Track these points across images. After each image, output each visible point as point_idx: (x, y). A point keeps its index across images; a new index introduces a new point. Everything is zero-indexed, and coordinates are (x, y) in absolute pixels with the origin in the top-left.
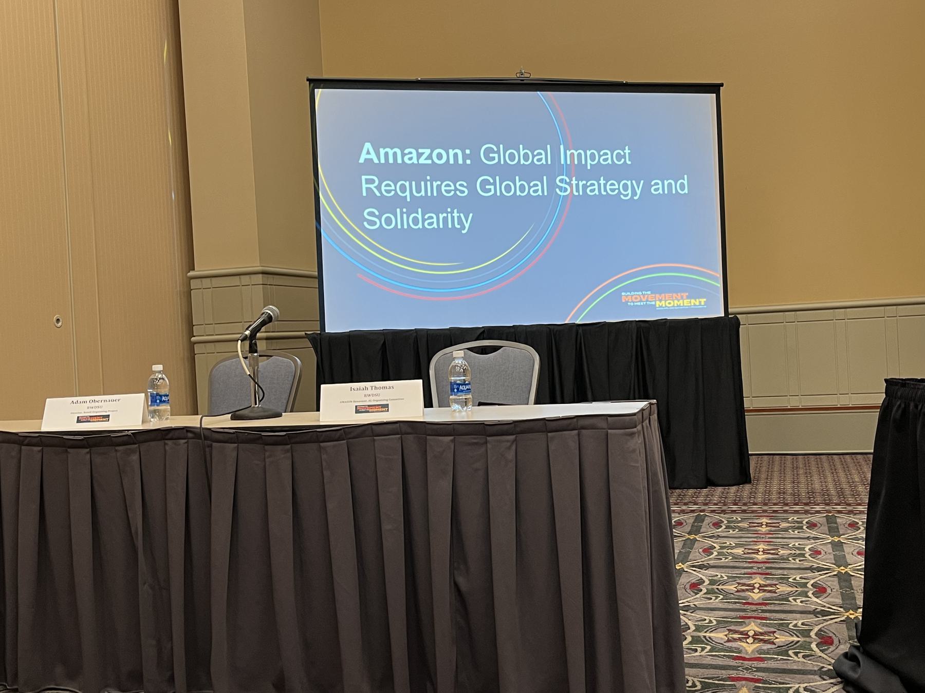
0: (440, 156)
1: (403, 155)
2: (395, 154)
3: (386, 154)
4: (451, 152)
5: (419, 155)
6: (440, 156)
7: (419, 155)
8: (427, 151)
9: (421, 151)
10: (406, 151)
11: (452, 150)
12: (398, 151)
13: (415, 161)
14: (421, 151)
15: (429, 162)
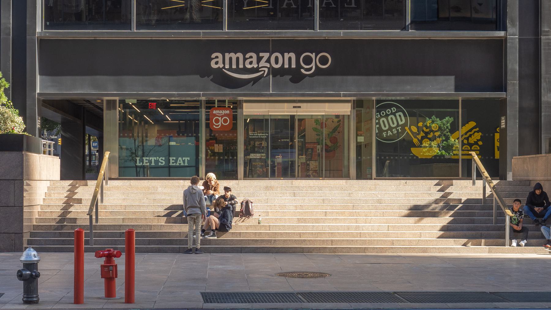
1: (245, 59)
2: (238, 59)
3: (231, 59)
8: (266, 55)
9: (261, 54)
10: (248, 56)
11: (287, 53)
12: (240, 55)
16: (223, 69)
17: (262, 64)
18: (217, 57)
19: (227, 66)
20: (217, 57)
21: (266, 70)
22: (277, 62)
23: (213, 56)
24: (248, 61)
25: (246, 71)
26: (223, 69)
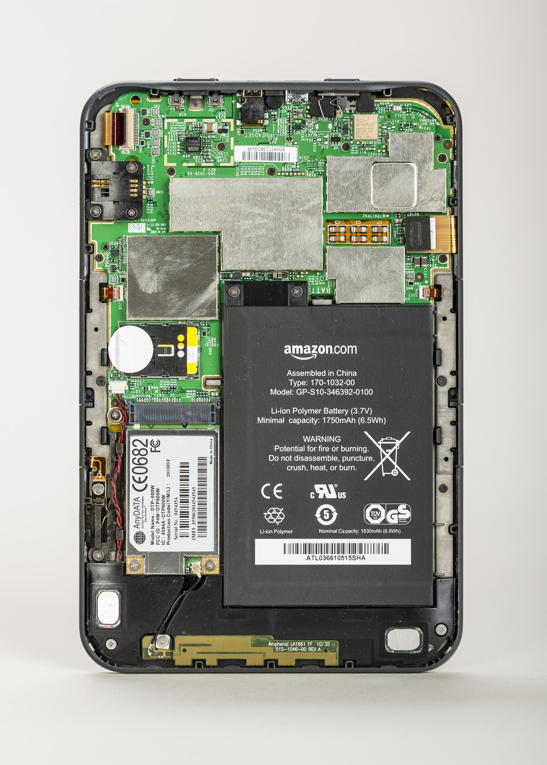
0: (322, 350)
1: (304, 349)
2: (300, 349)
3: (296, 349)
4: (327, 347)
5: (312, 349)
6: (322, 350)
7: (312, 349)
8: (315, 347)
9: (313, 346)
10: (305, 347)
12: (301, 347)
13: (309, 352)
14: (313, 346)
15: (317, 352)
16: (292, 355)
17: (314, 351)
18: (288, 348)
19: (294, 352)
20: (288, 348)
21: (316, 355)
22: (322, 350)
23: (286, 347)
24: (305, 350)
25: (304, 355)
26: (292, 355)
